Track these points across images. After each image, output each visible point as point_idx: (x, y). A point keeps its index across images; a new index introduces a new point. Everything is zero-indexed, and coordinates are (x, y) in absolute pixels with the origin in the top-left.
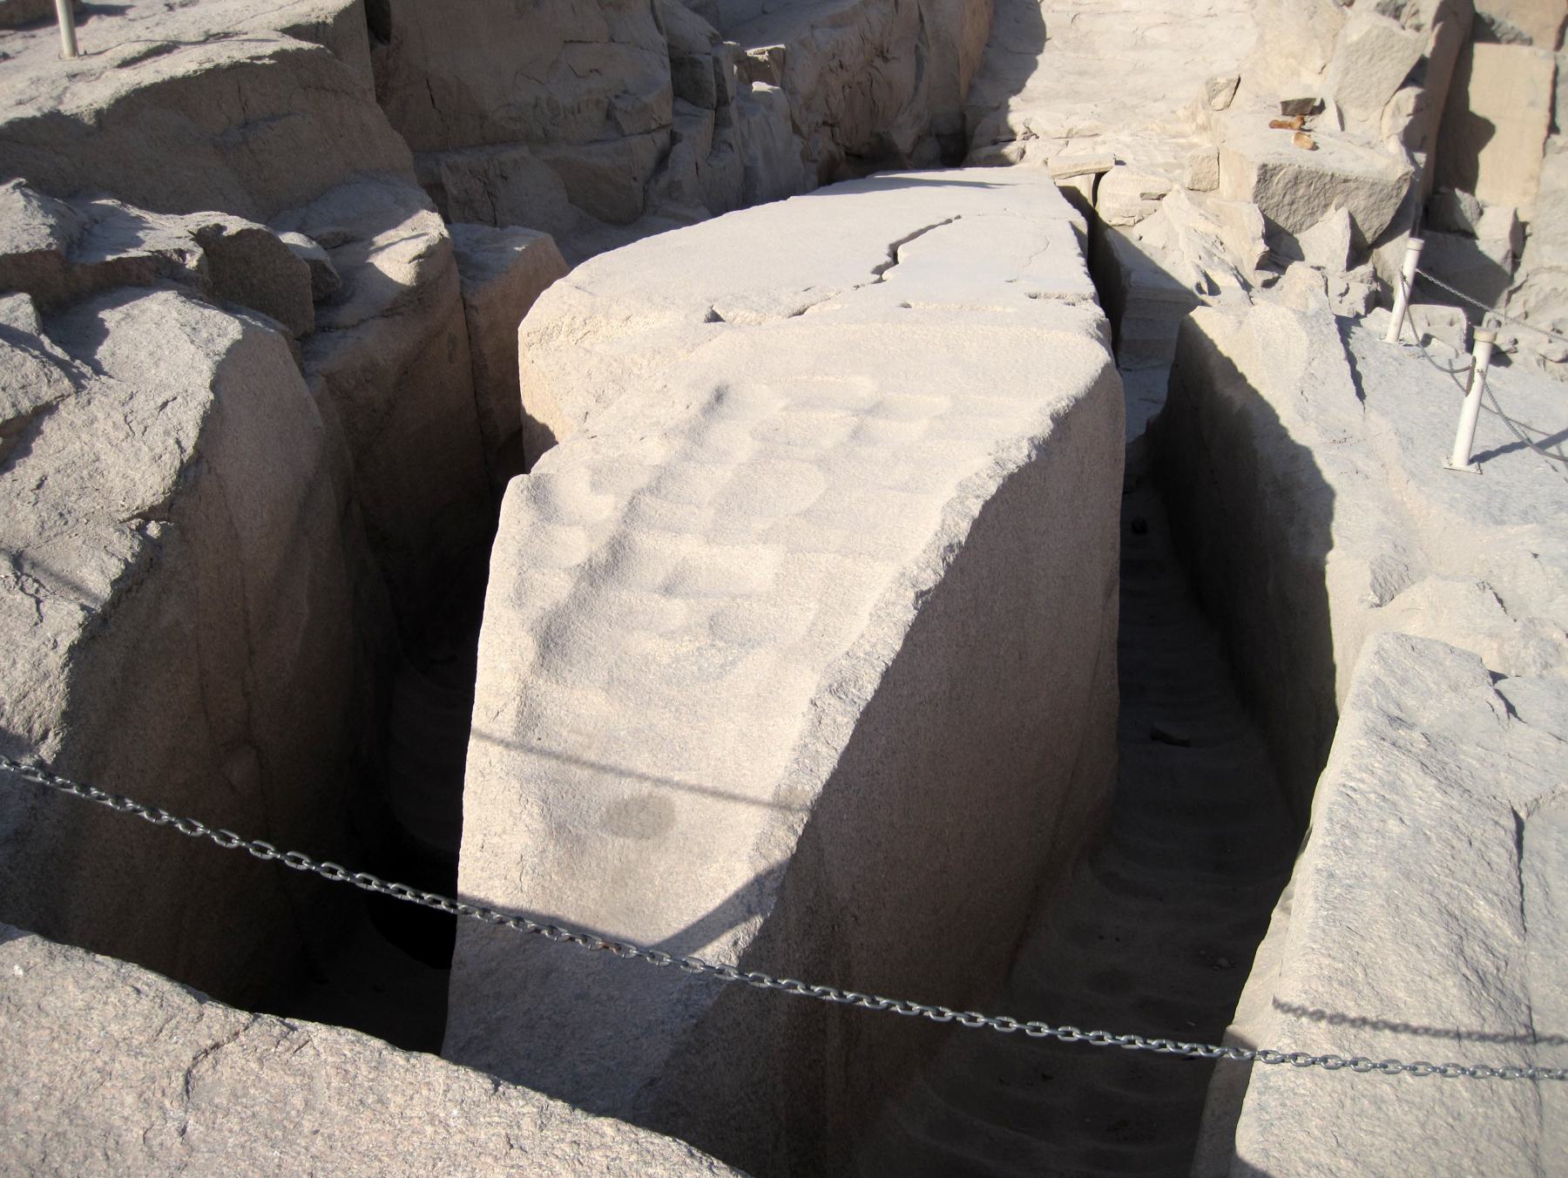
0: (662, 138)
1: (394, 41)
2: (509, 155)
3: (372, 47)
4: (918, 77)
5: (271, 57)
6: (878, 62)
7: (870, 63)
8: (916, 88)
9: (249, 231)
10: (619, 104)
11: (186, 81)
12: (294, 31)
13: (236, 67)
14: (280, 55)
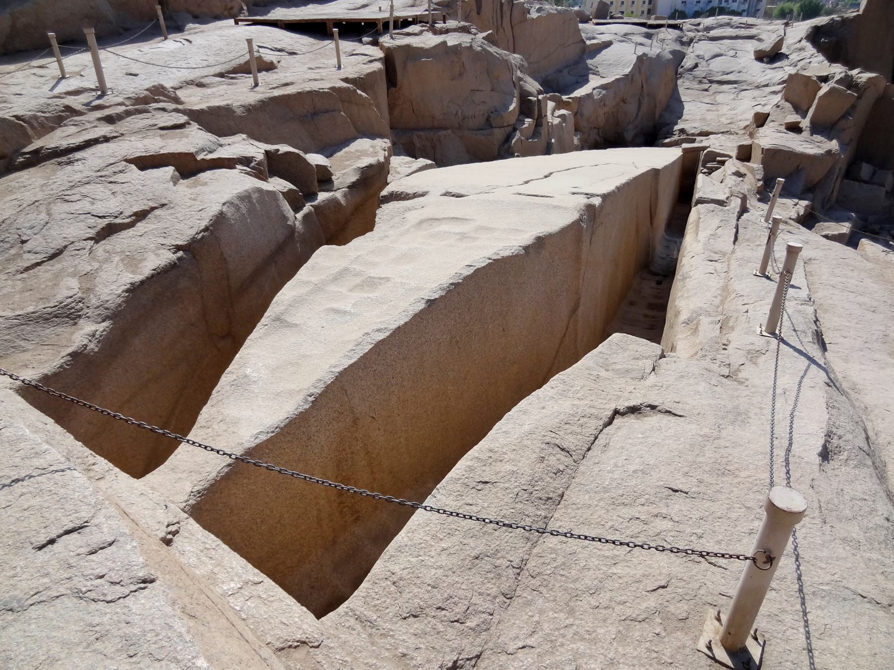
0: (510, 129)
1: (398, 87)
2: (444, 132)
3: (388, 89)
4: (639, 110)
5: (329, 89)
6: (622, 104)
7: (618, 105)
8: (637, 115)
9: (290, 152)
10: (492, 115)
11: (289, 96)
12: (346, 80)
13: (310, 93)
14: (333, 89)
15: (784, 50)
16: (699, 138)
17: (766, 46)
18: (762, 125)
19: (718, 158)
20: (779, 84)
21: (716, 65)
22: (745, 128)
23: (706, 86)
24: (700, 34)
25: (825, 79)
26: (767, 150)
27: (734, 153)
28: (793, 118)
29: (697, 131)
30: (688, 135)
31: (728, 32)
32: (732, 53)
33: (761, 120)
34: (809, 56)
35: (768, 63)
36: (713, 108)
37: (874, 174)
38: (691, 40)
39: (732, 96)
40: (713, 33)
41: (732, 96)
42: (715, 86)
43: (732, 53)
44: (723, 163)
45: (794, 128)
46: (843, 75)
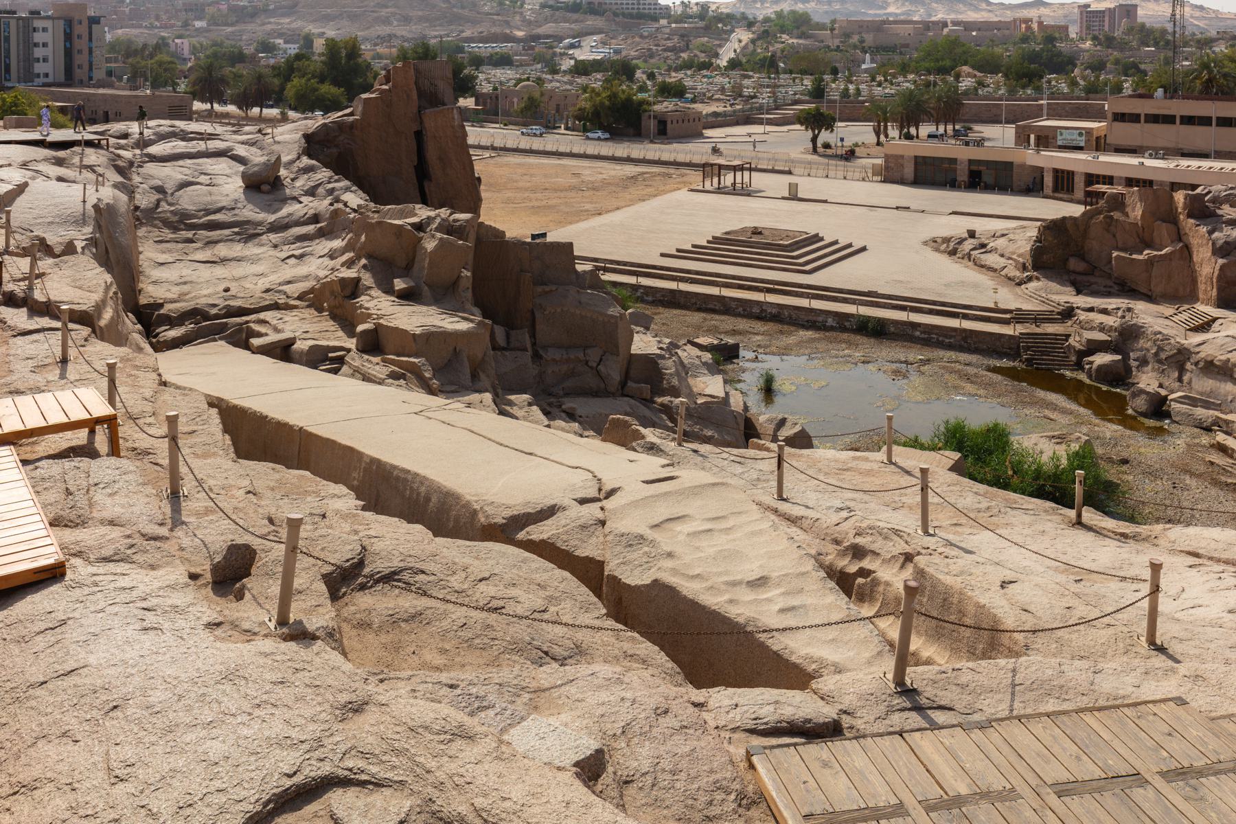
21: (188, 200)
27: (351, 343)
31: (180, 146)
32: (203, 179)
35: (268, 193)
37: (508, 336)
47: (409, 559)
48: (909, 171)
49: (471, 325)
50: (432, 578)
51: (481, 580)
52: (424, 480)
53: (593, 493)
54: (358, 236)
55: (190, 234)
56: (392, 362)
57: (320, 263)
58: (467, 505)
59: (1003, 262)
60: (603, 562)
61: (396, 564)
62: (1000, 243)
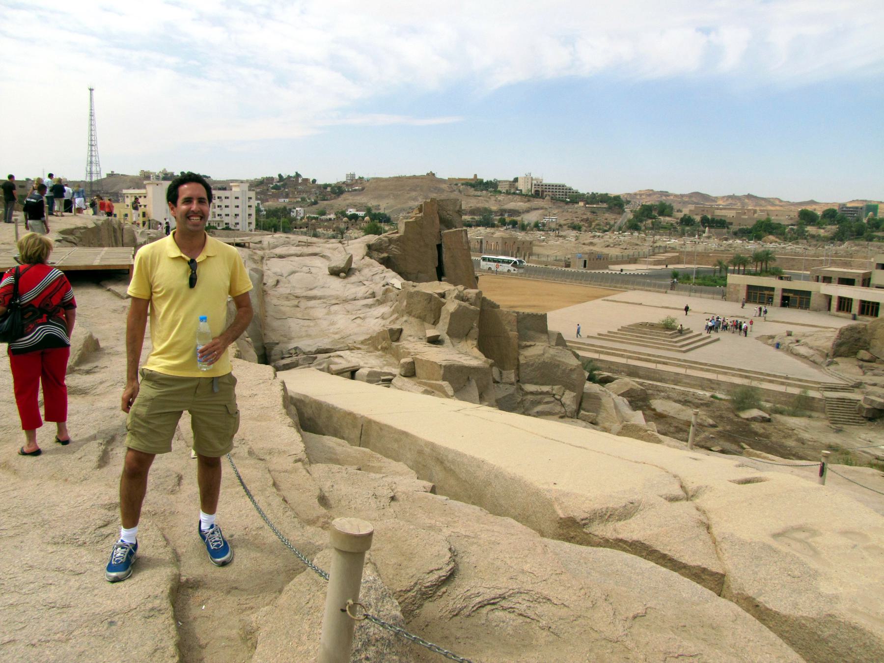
15: (353, 266)
16: (320, 356)
17: (339, 261)
18: (398, 340)
19: (382, 378)
20: (366, 298)
22: (362, 343)
23: (295, 302)
24: (267, 251)
25: (443, 295)
26: (445, 367)
27: (396, 371)
28: (431, 332)
29: (314, 349)
30: (304, 353)
31: (293, 250)
32: (305, 269)
33: (396, 335)
34: (380, 271)
35: (344, 278)
36: (312, 324)
38: (263, 258)
39: (326, 311)
40: (279, 251)
41: (326, 311)
42: (304, 304)
43: (305, 269)
44: (390, 380)
45: (435, 341)
46: (456, 292)
47: (521, 577)
48: (743, 294)
49: (480, 362)
50: (563, 612)
51: (635, 617)
52: (480, 464)
53: (677, 491)
54: (401, 303)
55: (295, 302)
56: (425, 384)
57: (375, 321)
58: (537, 493)
59: (811, 352)
60: (723, 576)
61: (503, 584)
62: (807, 340)
